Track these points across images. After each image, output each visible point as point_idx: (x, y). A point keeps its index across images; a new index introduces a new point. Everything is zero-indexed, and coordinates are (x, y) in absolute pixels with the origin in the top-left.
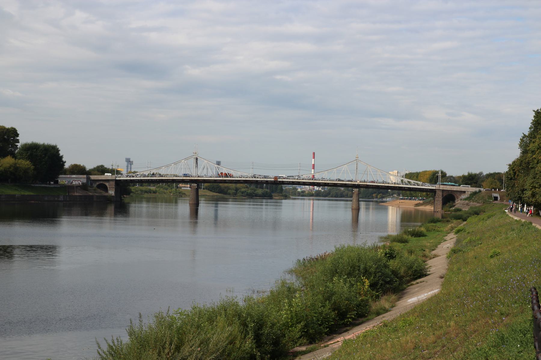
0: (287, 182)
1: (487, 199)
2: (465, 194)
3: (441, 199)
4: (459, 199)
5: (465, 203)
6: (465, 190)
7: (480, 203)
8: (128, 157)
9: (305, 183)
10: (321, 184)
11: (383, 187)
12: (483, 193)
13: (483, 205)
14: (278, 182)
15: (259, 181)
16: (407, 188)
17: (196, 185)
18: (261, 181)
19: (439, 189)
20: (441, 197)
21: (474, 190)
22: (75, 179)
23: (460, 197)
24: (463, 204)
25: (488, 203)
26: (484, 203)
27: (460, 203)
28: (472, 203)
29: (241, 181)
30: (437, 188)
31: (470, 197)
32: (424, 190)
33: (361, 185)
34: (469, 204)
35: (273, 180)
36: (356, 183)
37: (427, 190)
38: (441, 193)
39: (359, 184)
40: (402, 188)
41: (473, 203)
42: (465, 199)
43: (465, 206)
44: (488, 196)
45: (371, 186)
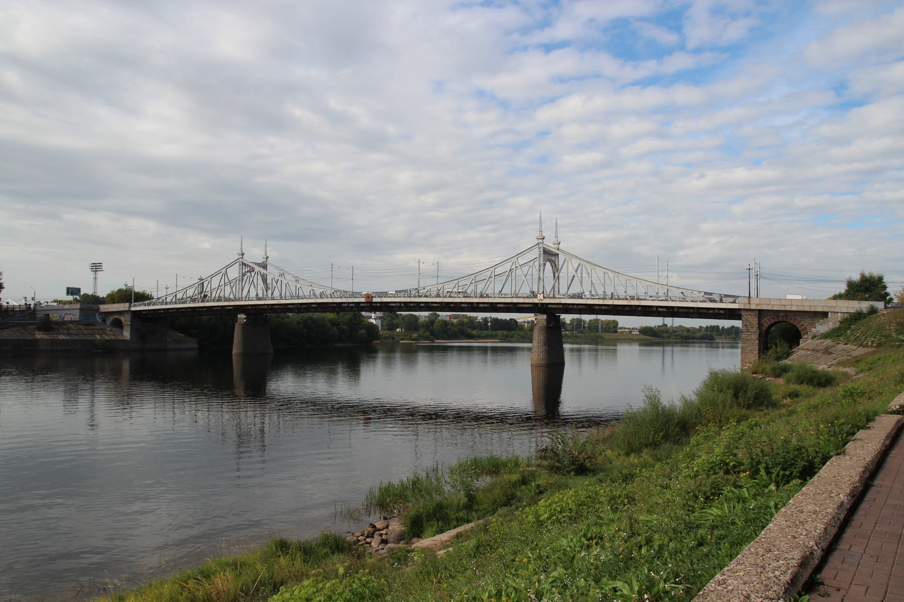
0: (395, 305)
1: (894, 335)
2: (825, 319)
3: (755, 337)
4: (810, 335)
5: (819, 348)
6: (826, 310)
7: (867, 346)
8: (104, 267)
9: (430, 305)
10: (464, 305)
11: (603, 307)
12: (883, 315)
13: (873, 353)
14: (378, 305)
15: (344, 305)
16: (665, 310)
17: (245, 317)
18: (347, 305)
19: (747, 307)
20: (755, 329)
21: (853, 308)
22: (67, 312)
23: (812, 329)
24: (813, 350)
25: (892, 347)
26: (880, 345)
27: (806, 348)
28: (841, 346)
29: (313, 306)
30: (742, 307)
31: (839, 328)
32: (711, 312)
33: (552, 306)
34: (831, 350)
35: (363, 300)
36: (536, 301)
37: (716, 311)
38: (754, 321)
39: (541, 302)
40: (652, 309)
41: (845, 346)
42: (825, 336)
43: (819, 354)
44: (898, 324)
45: (575, 307)
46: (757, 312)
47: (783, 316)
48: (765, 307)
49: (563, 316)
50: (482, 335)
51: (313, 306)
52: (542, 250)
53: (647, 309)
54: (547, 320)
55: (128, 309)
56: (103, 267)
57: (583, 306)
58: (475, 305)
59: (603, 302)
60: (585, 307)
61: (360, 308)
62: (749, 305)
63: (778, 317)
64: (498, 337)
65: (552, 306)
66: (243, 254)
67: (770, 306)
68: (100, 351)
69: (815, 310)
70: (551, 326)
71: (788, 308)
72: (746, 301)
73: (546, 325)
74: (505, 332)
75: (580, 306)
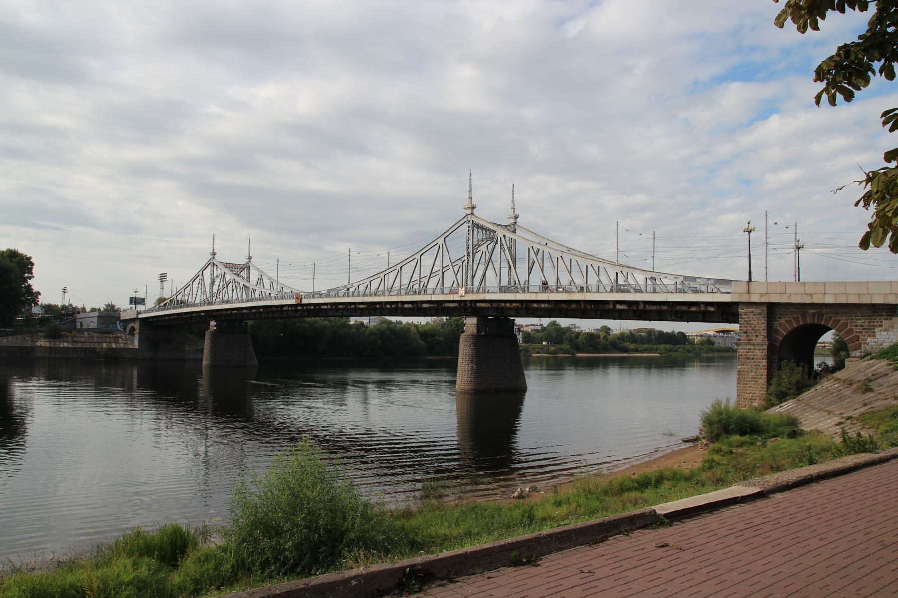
3: (760, 353)
9: (358, 307)
19: (745, 299)
20: (760, 340)
23: (869, 340)
30: (736, 299)
32: (694, 309)
38: (760, 324)
39: (463, 299)
40: (607, 307)
46: (765, 309)
47: (814, 315)
48: (775, 299)
49: (519, 321)
50: (640, 349)
53: (601, 307)
54: (478, 324)
55: (135, 317)
56: (167, 277)
59: (537, 296)
62: (748, 295)
63: (804, 317)
64: (658, 351)
65: (483, 305)
67: (785, 296)
68: (102, 359)
69: (869, 302)
70: (483, 334)
71: (817, 300)
72: (744, 288)
74: (667, 346)
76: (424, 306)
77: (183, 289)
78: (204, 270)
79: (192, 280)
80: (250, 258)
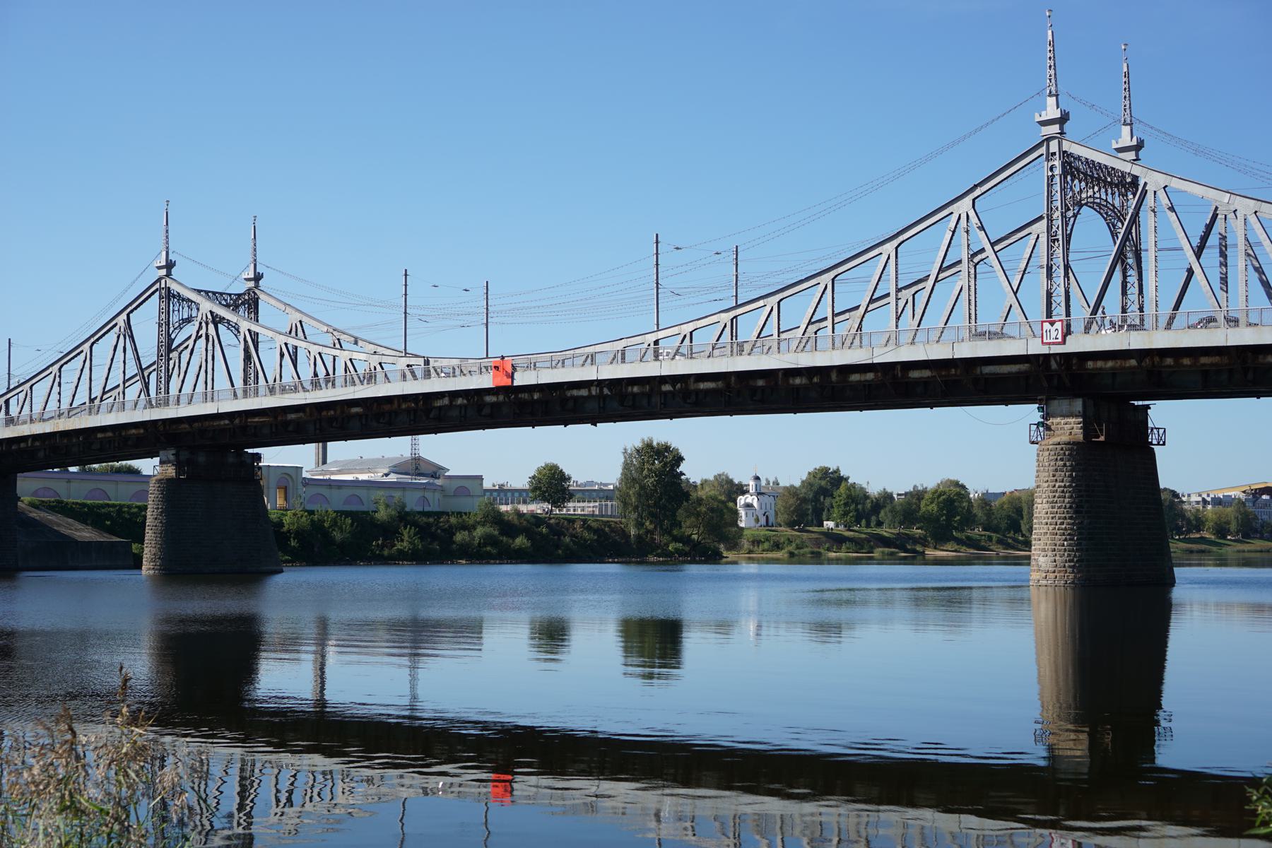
0: (584, 392)
9: (692, 386)
18: (446, 401)
29: (355, 410)
36: (1036, 348)
51: (355, 410)
52: (1057, 163)
57: (1216, 359)
58: (834, 376)
60: (1225, 360)
61: (486, 411)
66: (170, 266)
70: (1102, 438)
73: (1080, 438)
75: (1204, 360)
76: (915, 374)
77: (57, 366)
78: (132, 311)
79: (92, 340)
80: (258, 278)
